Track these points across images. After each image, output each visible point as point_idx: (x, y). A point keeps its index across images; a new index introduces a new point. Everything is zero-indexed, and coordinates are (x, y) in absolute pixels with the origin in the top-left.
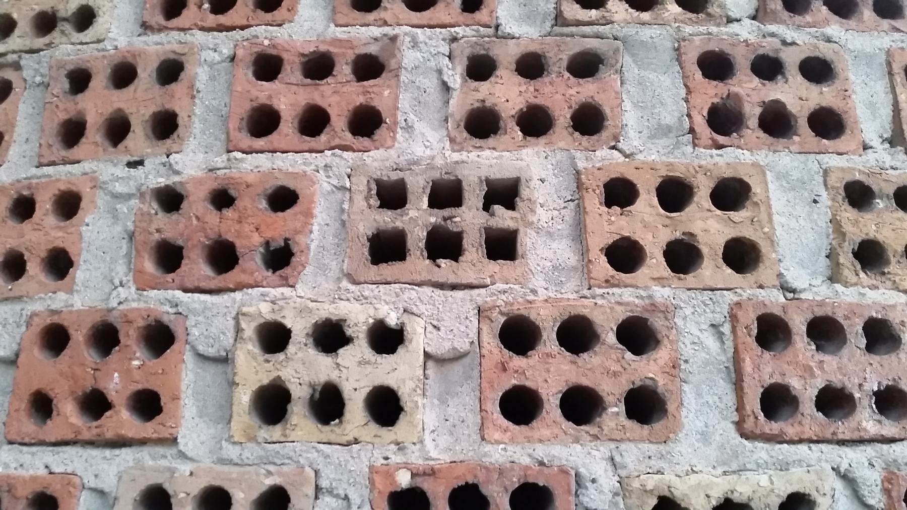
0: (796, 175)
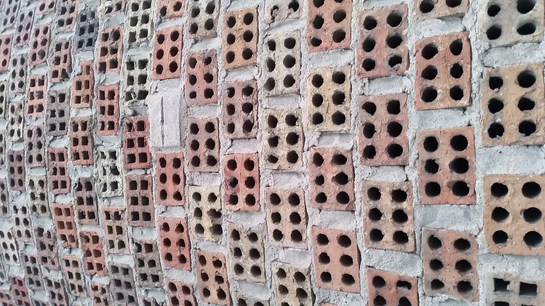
0: (487, 159)
